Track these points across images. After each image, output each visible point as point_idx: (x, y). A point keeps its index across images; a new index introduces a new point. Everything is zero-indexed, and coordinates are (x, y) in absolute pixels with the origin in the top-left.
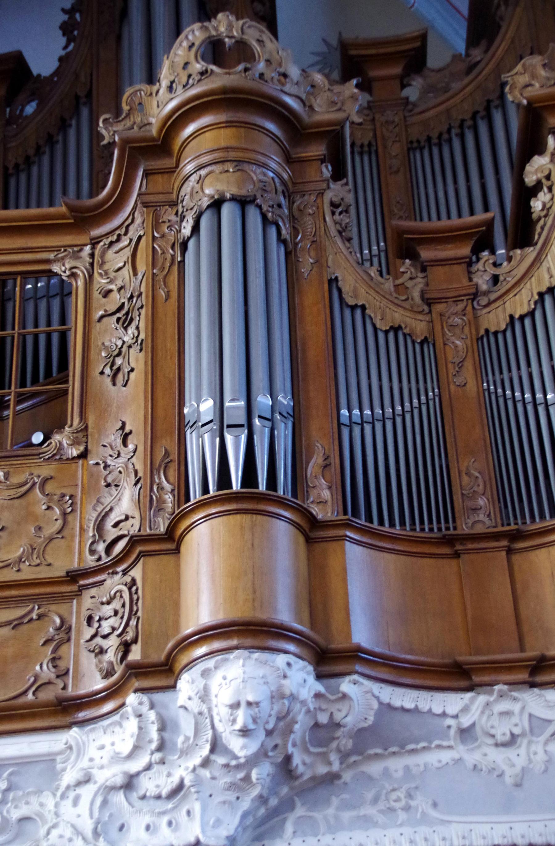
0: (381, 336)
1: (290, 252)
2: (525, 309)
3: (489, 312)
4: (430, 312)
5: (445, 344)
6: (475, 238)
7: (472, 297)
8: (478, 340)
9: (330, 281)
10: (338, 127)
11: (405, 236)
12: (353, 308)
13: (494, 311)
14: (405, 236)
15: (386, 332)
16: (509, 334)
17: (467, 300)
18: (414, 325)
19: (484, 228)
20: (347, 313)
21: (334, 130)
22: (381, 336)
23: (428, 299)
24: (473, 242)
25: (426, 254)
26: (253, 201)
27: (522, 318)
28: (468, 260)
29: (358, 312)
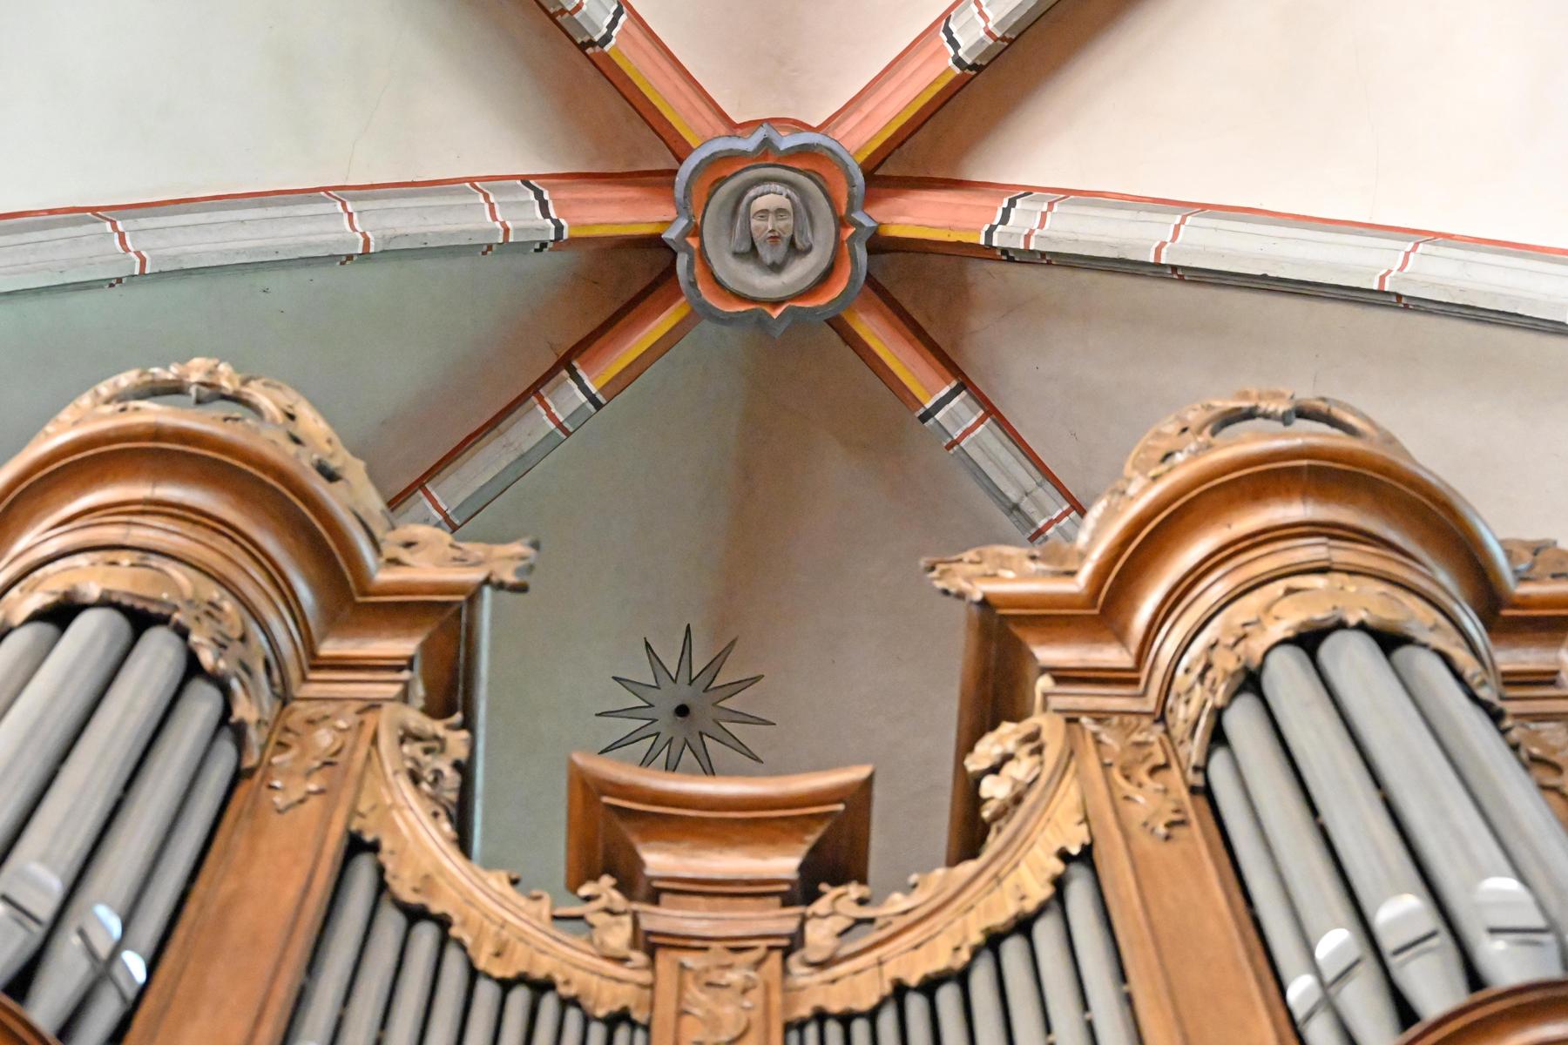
0: (486, 993)
1: (251, 772)
2: (940, 958)
3: (834, 981)
4: (652, 965)
5: (682, 1013)
6: (811, 839)
7: (784, 942)
8: (788, 1027)
9: (356, 846)
10: (461, 598)
11: (605, 799)
12: (415, 915)
13: (848, 979)
14: (605, 799)
15: (506, 985)
16: (887, 1020)
17: (771, 948)
18: (594, 987)
19: (841, 807)
20: (391, 924)
21: (448, 604)
22: (486, 993)
23: (650, 933)
24: (804, 849)
25: (658, 861)
26: (162, 620)
27: (929, 987)
28: (785, 887)
29: (426, 935)
